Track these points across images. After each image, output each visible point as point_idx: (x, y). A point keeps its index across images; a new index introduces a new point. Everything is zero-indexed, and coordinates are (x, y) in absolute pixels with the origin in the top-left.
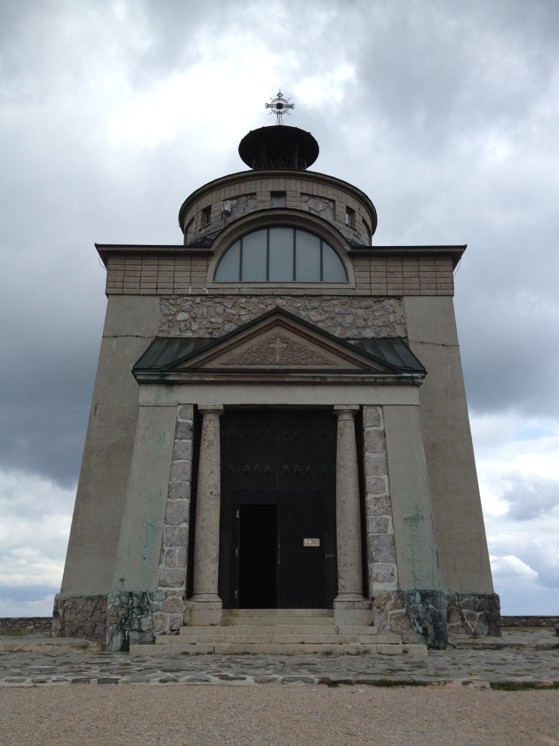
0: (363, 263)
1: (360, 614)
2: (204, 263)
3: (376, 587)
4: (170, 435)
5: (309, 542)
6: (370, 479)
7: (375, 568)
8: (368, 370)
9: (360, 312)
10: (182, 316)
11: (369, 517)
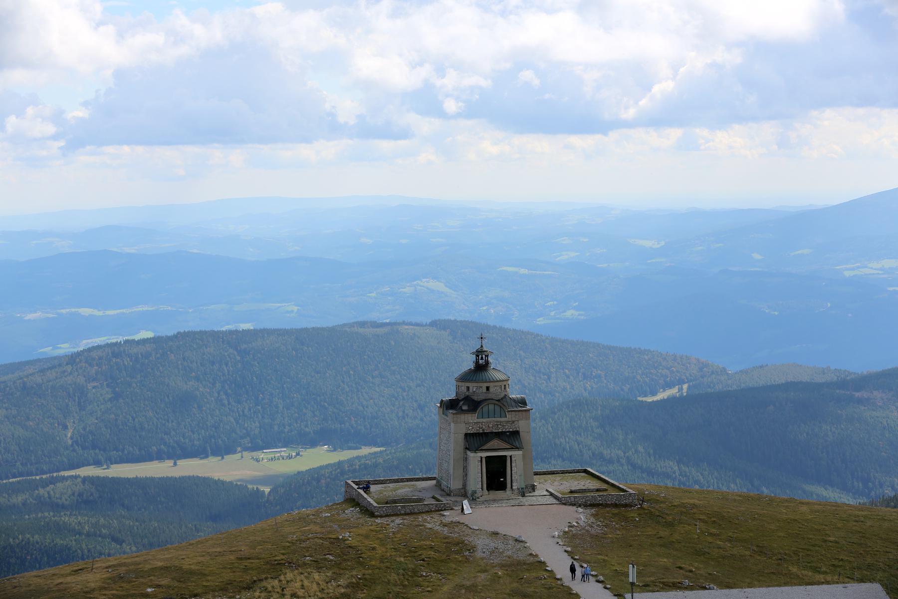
0: (510, 413)
1: (511, 492)
2: (474, 414)
3: (514, 488)
4: (477, 463)
5: (501, 480)
6: (513, 469)
7: (514, 484)
8: (513, 448)
9: (509, 425)
10: (470, 428)
11: (513, 476)
